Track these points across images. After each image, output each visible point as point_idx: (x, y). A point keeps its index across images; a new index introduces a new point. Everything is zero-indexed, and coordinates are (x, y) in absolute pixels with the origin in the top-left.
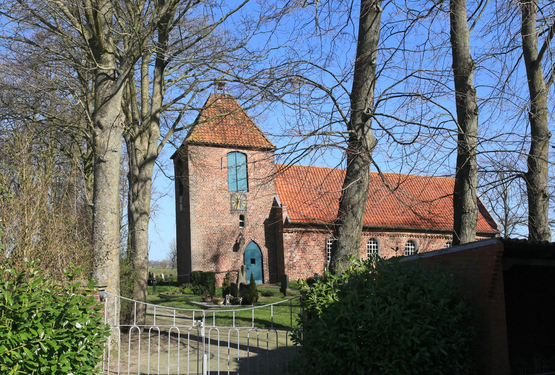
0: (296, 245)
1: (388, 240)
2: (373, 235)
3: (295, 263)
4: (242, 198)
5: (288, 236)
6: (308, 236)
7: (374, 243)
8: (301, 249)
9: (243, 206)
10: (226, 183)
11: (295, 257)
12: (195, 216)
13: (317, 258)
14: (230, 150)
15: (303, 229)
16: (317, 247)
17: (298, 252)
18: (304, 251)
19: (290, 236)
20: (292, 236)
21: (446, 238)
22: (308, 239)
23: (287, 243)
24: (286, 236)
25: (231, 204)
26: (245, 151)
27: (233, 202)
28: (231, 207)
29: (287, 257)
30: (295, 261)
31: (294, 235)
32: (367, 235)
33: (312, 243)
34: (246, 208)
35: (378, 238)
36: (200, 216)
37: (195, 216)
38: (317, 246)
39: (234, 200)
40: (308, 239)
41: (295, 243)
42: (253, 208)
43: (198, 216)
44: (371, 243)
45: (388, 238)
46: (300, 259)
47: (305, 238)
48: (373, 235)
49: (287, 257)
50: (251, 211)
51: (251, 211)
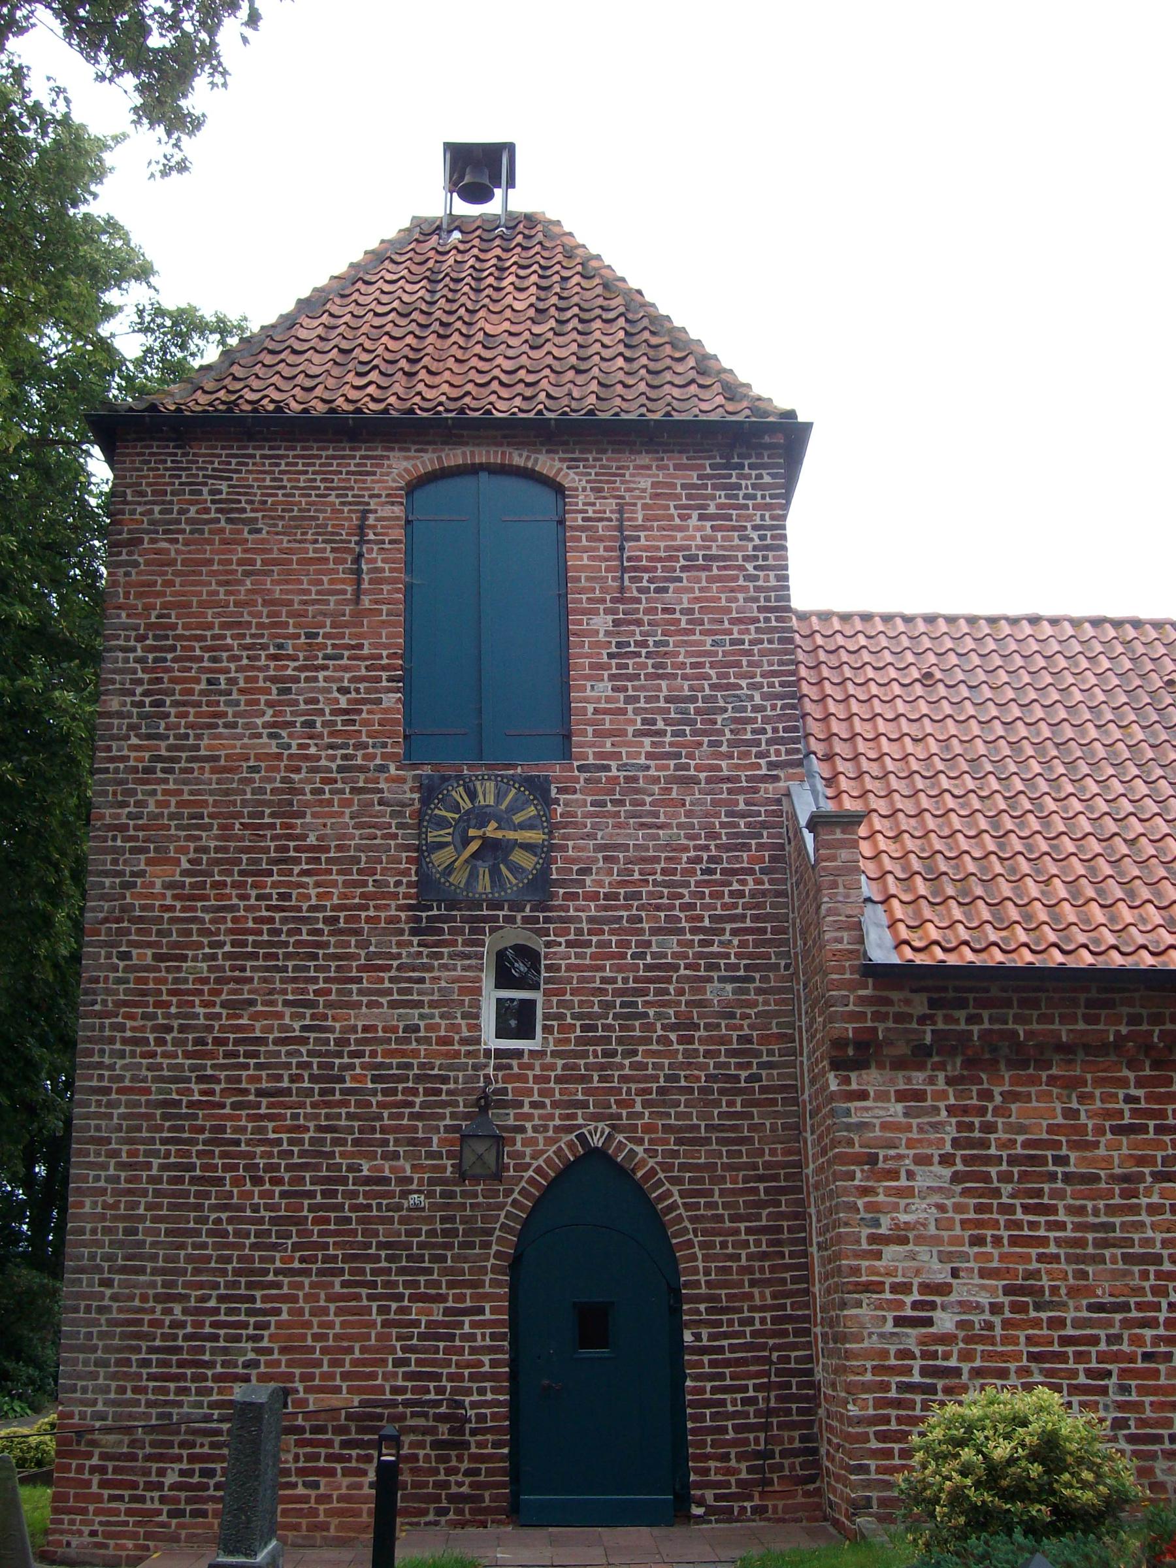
0: (956, 1178)
4: (513, 809)
5: (882, 1096)
6: (1072, 1084)
8: (1007, 1209)
9: (515, 869)
10: (391, 700)
11: (943, 1289)
12: (125, 956)
14: (426, 461)
17: (978, 1241)
19: (901, 1096)
20: (919, 1096)
23: (872, 1159)
24: (863, 1095)
25: (422, 852)
26: (547, 464)
27: (433, 836)
30: (945, 1322)
36: (157, 957)
37: (125, 956)
39: (442, 823)
41: (946, 1160)
42: (599, 881)
46: (995, 1309)
50: (586, 912)
51: (586, 912)
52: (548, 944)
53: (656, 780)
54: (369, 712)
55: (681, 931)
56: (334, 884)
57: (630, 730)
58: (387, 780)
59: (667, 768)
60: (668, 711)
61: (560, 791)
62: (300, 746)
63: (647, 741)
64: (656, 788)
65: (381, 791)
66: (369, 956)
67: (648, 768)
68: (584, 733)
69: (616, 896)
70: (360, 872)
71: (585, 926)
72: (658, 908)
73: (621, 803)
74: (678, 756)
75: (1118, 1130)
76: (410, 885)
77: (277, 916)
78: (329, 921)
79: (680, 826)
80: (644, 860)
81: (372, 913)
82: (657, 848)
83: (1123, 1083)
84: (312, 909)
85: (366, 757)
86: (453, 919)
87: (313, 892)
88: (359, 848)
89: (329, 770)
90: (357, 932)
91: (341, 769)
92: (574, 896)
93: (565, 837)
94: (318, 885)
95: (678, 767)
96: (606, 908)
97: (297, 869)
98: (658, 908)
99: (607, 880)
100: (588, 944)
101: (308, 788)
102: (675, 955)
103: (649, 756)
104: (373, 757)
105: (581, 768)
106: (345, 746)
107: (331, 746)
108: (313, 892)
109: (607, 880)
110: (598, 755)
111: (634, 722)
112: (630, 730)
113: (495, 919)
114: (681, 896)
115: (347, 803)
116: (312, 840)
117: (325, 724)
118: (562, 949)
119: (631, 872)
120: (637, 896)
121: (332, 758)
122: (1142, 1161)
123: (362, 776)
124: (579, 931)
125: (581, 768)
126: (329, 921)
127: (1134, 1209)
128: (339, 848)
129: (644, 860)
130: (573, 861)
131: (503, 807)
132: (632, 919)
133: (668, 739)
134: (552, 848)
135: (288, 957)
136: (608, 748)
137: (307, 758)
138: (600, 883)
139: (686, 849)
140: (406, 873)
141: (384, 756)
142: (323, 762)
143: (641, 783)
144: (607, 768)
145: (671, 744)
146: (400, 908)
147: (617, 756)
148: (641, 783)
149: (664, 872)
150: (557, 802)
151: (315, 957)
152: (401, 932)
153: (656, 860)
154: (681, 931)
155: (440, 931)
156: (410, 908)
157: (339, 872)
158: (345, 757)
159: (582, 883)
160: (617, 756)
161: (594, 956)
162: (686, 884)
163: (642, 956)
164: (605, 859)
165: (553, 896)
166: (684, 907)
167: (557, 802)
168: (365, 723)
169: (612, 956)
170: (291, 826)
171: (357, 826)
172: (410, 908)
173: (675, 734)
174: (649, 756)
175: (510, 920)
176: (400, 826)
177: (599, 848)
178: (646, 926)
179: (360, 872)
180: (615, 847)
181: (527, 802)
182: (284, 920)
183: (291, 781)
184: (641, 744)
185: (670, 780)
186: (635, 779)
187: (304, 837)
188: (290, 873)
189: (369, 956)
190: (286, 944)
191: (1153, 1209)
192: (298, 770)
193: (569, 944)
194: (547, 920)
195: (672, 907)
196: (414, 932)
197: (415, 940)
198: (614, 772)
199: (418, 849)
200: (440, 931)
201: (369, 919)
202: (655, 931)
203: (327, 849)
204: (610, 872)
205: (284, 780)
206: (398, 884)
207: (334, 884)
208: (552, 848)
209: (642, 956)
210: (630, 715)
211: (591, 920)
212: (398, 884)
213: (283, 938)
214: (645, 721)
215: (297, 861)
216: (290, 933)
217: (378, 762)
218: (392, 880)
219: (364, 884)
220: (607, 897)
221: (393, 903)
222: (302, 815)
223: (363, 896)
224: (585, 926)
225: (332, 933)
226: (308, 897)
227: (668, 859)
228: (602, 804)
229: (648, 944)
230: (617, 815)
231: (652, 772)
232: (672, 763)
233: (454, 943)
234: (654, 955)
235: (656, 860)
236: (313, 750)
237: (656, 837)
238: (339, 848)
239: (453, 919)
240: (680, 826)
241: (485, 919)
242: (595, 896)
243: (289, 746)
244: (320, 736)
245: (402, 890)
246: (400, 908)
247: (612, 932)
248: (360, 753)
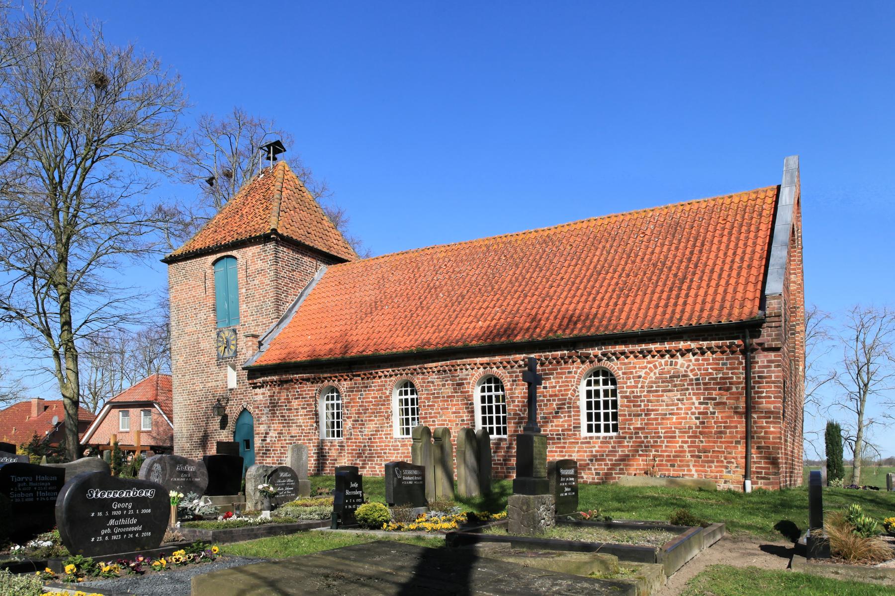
0: (270, 411)
1: (433, 382)
2: (401, 374)
3: (269, 444)
6: (287, 389)
7: (605, 383)
13: (302, 433)
15: (275, 378)
16: (302, 412)
18: (287, 422)
21: (584, 359)
22: (288, 395)
27: (220, 344)
28: (218, 355)
29: (258, 434)
30: (268, 440)
31: (266, 391)
32: (391, 376)
33: (295, 403)
34: (236, 352)
35: (417, 381)
38: (303, 408)
40: (288, 395)
41: (268, 407)
43: (180, 376)
44: (490, 389)
45: (433, 377)
46: (276, 437)
47: (284, 395)
48: (404, 372)
49: (258, 434)
75: (296, 399)
83: (296, 388)
122: (299, 405)
127: (298, 416)
185: (256, 325)
191: (301, 415)
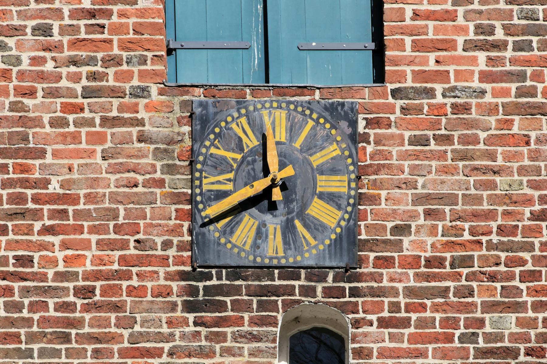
52: (357, 324)
53: (492, 110)
54: (122, 15)
55: (519, 307)
56: (87, 245)
57: (460, 41)
58: (147, 107)
59: (506, 93)
60: (509, 15)
61: (369, 123)
62: (35, 61)
63: (482, 56)
64: (492, 120)
65: (141, 123)
66: (133, 339)
67: (483, 92)
68: (400, 45)
69: (440, 262)
70: (118, 229)
71: (402, 300)
72: (493, 277)
73: (447, 139)
74: (521, 76)
76: (181, 247)
77: (16, 285)
78: (79, 292)
79: (522, 171)
80: (476, 215)
81: (135, 282)
82: (493, 200)
84: (60, 276)
85: (118, 77)
86: (237, 290)
87: (60, 255)
88: (114, 198)
89: (72, 93)
90: (117, 307)
91: (88, 93)
92: (388, 262)
93: (375, 185)
94: (65, 246)
95: (521, 93)
96: (428, 278)
97: (38, 226)
98: (493, 277)
99: (430, 240)
100: (405, 323)
101: (46, 118)
102: (514, 337)
103: (485, 77)
104: (129, 76)
105: (395, 93)
106: (92, 61)
107: (74, 62)
108: (60, 255)
109: (430, 240)
110: (418, 76)
111: (464, 30)
112: (460, 41)
113: (290, 291)
114: (523, 262)
115: (100, 138)
116: (54, 187)
117: (63, 31)
118: (373, 329)
119: (459, 231)
120: (466, 262)
121: (76, 77)
123: (116, 102)
124: (395, 307)
125: (395, 93)
126: (79, 292)
128: (90, 198)
129: (476, 215)
130: (386, 217)
131: (297, 145)
132: (460, 292)
133: (509, 53)
134: (360, 198)
135: (32, 338)
136: (432, 66)
137: (42, 77)
138: (421, 245)
139: (529, 201)
140: (175, 231)
141: (143, 75)
142: (64, 83)
143: (474, 114)
144: (430, 93)
145: (513, 61)
146: (169, 277)
147: (443, 76)
148: (474, 114)
149: (501, 230)
150: (365, 138)
151: (66, 338)
152: (173, 307)
153: (490, 215)
154: (519, 307)
155: (222, 306)
156: (183, 276)
157: (93, 230)
158: (93, 76)
159: (398, 246)
160: (443, 76)
161: (413, 339)
162: (530, 247)
163: (473, 338)
164: (428, 214)
165: (361, 262)
166: (526, 277)
167: (365, 138)
168: (117, 29)
169: (435, 339)
170: (25, 169)
171: (114, 170)
172: (183, 276)
173: (518, 47)
174: (485, 77)
175: (308, 291)
176: (170, 169)
177: (418, 200)
178: (477, 300)
179: (118, 229)
180: (441, 199)
181: (329, 139)
182: (26, 291)
183: (23, 108)
184: (474, 61)
186: (466, 108)
187: (46, 183)
188: (29, 231)
189: (133, 339)
190: (29, 322)
192: (32, 93)
193: (383, 323)
194: (355, 292)
195: (511, 277)
196: (189, 307)
197: (191, 317)
198: (439, 99)
199: (191, 200)
200: (222, 306)
201: (131, 291)
202: (489, 307)
203: (74, 200)
204: (433, 231)
205: (14, 107)
206: (167, 245)
207: (87, 245)
208: (360, 198)
209: (473, 338)
210: (460, 20)
211: (410, 292)
212: (167, 245)
213: (25, 313)
214: (479, 30)
215: (37, 215)
216: (33, 308)
217: (135, 82)
218: (159, 241)
219: (124, 245)
220: (429, 263)
221: (162, 271)
222: (41, 154)
223: (123, 260)
224: (402, 300)
225: (87, 308)
226: (54, 262)
227: (506, 214)
228: (423, 141)
229: (481, 323)
230: (442, 156)
231: (488, 98)
232: (513, 87)
233: (239, 321)
234: (488, 338)
235: (490, 215)
236: (49, 66)
237: (492, 185)
238: (90, 198)
239: (237, 290)
240: (522, 171)
241: (276, 291)
242: (414, 262)
243: (18, 61)
244: (58, 47)
245: (172, 252)
246: (169, 277)
247: (436, 308)
248: (111, 71)
